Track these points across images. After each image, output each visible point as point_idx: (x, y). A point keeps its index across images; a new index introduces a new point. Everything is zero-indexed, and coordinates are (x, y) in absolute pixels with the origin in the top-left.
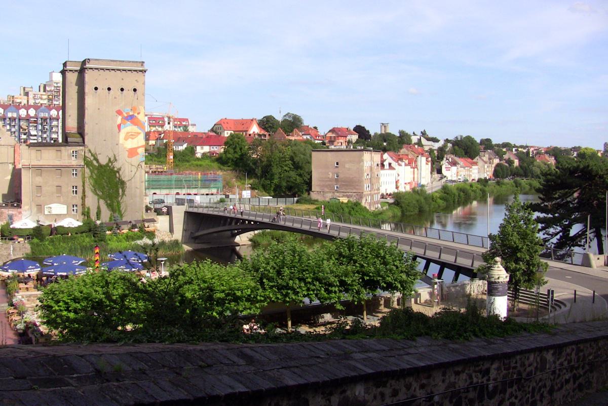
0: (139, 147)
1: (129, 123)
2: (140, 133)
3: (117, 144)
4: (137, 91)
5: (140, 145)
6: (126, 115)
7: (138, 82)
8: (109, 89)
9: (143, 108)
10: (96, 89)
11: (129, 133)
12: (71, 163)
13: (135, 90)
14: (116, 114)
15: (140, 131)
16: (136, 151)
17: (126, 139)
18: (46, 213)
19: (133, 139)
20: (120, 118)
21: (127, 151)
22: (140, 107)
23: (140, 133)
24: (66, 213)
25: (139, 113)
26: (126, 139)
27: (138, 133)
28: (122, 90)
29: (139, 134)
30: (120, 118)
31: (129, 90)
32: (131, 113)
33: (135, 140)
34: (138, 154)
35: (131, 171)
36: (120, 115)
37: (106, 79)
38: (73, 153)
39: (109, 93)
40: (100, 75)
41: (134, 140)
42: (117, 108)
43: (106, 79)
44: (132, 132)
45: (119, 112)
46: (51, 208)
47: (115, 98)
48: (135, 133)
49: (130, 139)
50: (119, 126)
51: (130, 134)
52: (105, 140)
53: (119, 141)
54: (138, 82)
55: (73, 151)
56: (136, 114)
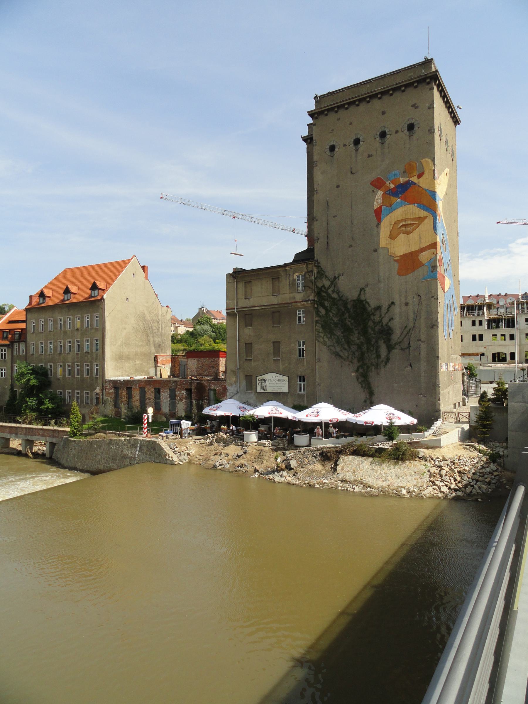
0: (422, 250)
1: (399, 200)
2: (425, 218)
3: (375, 251)
4: (416, 129)
5: (423, 245)
6: (392, 186)
7: (417, 107)
8: (357, 142)
9: (429, 160)
10: (332, 148)
11: (401, 221)
12: (294, 298)
13: (411, 127)
14: (372, 188)
15: (423, 213)
16: (418, 256)
17: (392, 237)
18: (259, 389)
19: (408, 233)
20: (380, 193)
21: (395, 260)
22: (423, 161)
23: (425, 218)
24: (286, 390)
25: (420, 176)
26: (392, 237)
27: (419, 218)
28: (383, 135)
29: (421, 220)
30: (380, 193)
31: (397, 132)
32: (403, 180)
33: (414, 236)
34: (421, 264)
35: (407, 304)
36: (379, 188)
37: (351, 124)
38: (298, 280)
39: (357, 150)
40: (339, 119)
41: (409, 236)
42: (373, 176)
43: (351, 124)
44: (405, 220)
45: (378, 184)
46: (265, 380)
47: (369, 156)
48: (413, 219)
49: (402, 236)
50: (378, 213)
51: (401, 224)
52: (350, 246)
53: (378, 244)
54: (417, 107)
55: (298, 277)
56: (414, 179)
